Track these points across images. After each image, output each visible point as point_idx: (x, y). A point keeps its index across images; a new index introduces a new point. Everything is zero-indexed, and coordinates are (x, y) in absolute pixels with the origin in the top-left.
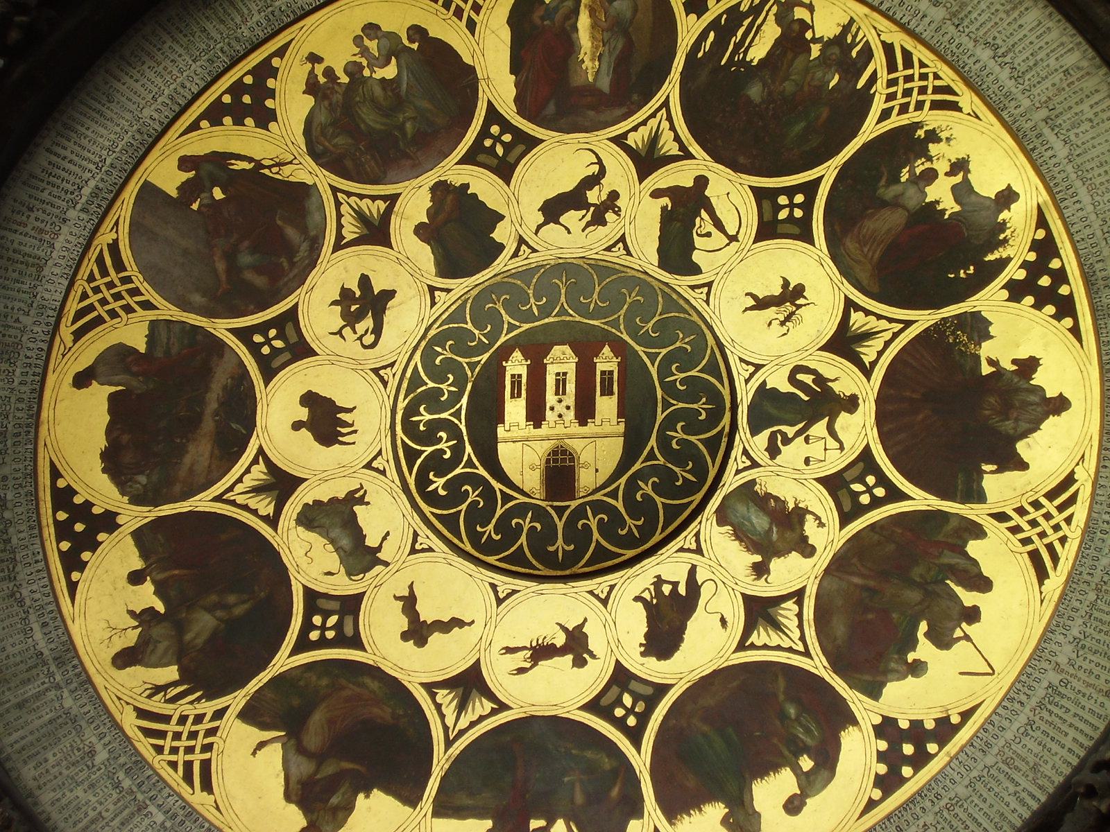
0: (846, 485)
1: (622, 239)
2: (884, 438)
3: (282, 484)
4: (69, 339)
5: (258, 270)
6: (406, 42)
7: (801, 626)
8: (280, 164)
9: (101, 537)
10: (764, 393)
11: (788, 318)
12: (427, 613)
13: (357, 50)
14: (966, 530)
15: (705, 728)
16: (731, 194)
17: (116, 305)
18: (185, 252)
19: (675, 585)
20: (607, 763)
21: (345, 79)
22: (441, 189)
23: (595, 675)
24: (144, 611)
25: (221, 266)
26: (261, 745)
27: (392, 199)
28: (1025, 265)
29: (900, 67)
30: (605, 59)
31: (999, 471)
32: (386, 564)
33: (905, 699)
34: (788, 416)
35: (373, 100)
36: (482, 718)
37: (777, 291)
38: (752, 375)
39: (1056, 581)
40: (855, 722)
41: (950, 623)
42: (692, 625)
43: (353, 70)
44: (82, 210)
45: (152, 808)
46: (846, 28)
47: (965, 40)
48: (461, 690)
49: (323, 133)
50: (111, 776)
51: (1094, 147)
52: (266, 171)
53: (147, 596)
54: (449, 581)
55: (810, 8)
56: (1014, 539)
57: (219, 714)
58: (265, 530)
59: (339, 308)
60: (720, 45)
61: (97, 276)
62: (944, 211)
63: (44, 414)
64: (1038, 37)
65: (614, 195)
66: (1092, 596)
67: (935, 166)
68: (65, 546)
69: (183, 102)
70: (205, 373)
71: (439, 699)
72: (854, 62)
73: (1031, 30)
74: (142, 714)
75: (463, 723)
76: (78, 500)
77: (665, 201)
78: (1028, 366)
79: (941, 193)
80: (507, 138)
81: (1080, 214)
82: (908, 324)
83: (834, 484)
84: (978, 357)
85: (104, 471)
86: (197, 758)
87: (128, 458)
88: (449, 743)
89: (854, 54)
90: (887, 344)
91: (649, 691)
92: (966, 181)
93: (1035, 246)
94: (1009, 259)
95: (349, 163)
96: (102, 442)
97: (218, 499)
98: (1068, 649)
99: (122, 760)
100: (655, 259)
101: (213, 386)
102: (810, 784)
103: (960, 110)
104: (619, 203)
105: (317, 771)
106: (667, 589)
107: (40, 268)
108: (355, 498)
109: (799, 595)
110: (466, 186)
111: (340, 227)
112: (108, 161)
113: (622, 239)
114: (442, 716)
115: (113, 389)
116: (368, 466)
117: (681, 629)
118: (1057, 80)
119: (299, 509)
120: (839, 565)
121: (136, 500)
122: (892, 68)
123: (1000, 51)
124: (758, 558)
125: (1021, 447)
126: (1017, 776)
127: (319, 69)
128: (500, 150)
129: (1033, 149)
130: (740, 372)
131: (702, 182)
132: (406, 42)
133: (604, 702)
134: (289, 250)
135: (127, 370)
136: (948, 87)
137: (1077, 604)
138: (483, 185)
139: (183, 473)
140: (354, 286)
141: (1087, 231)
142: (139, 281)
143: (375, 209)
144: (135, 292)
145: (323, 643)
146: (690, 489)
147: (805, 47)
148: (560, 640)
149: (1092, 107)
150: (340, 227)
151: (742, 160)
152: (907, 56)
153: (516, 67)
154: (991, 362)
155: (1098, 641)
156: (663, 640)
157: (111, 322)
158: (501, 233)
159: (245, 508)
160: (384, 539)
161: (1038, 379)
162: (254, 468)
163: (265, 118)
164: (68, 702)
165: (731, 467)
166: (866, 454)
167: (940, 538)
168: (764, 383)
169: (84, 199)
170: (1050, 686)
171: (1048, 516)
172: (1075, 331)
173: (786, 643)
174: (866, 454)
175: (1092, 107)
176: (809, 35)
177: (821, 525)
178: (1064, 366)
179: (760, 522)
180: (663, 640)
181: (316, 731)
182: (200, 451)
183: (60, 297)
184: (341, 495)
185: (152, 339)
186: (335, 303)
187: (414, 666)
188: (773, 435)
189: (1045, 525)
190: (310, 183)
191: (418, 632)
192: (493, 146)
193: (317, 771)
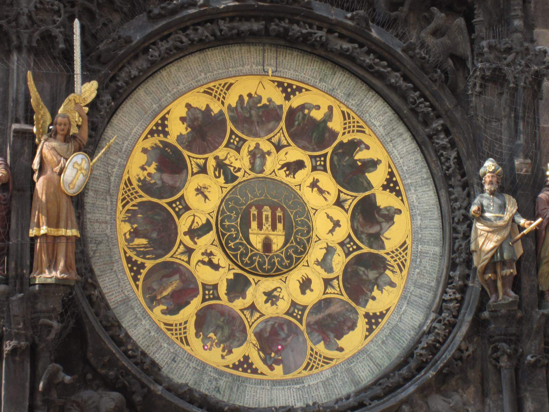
0: (236, 146)
1: (212, 244)
2: (220, 144)
3: (327, 283)
4: (334, 361)
5: (283, 330)
6: (202, 336)
7: (276, 134)
9: (371, 314)
10: (226, 182)
11: (205, 188)
12: (331, 225)
13: (213, 348)
14: (230, 109)
15: (313, 141)
16: (183, 224)
18: (292, 351)
19: (285, 171)
20: (335, 158)
21: (222, 345)
22: (231, 300)
24: (379, 290)
25: (289, 340)
26: (387, 239)
27: (242, 310)
28: (159, 136)
29: (126, 200)
30: (171, 281)
31: (212, 110)
32: (327, 244)
33: (278, 98)
34: (229, 172)
35: (222, 334)
36: (345, 194)
37: (200, 195)
38: (224, 188)
39: (231, 81)
40: (290, 106)
41: (254, 99)
43: (218, 345)
44: (303, 383)
45: (419, 250)
46: (125, 221)
49: (239, 341)
50: (420, 265)
53: (376, 292)
54: (320, 225)
55: (125, 234)
56: (226, 97)
57: (388, 254)
58: (341, 278)
59: (278, 303)
60: (148, 253)
61: (315, 367)
62: (156, 165)
63: (356, 351)
65: (203, 254)
66: (230, 69)
67: (146, 175)
68: (380, 320)
70: (316, 323)
71: (348, 207)
72: (132, 214)
74: (401, 270)
75: (349, 197)
76: (368, 326)
77: (196, 240)
78: (183, 119)
79: (152, 169)
82: (189, 157)
83: (238, 149)
84: (188, 134)
85: (356, 326)
86: (401, 250)
87: (349, 324)
88: (356, 197)
89: (130, 215)
90: (197, 158)
91: (313, 160)
92: (146, 164)
95: (241, 328)
96: (351, 332)
97: (342, 295)
98: (246, 67)
99: (414, 265)
100: (211, 232)
101: (317, 318)
102: (312, 107)
103: (129, 177)
104: (203, 251)
105: (383, 222)
106: (287, 172)
107: (325, 382)
108: (318, 263)
109: (269, 140)
110: (226, 294)
111: (258, 318)
112: (287, 387)
113: (212, 244)
114: (351, 203)
115: (337, 341)
116: (308, 266)
117: (294, 162)
119: (330, 274)
120: (256, 135)
121: (357, 313)
122: (128, 202)
124: (267, 156)
125: (203, 109)
126: (281, 61)
127: (224, 354)
128: (211, 292)
130: (225, 191)
131: (185, 234)
132: (202, 336)
133: (322, 168)
134: (273, 326)
135: (330, 341)
138: (222, 290)
139: (343, 308)
140: (269, 304)
141: (143, 124)
142: (308, 356)
143: (247, 313)
144: (311, 355)
145: (355, 244)
146: (223, 221)
147: (135, 229)
148: (315, 189)
150: (258, 318)
151: (173, 227)
152: (123, 200)
153: (188, 303)
156: (300, 165)
157: (323, 355)
158: (231, 276)
159: (339, 287)
160: (322, 249)
161: (184, 115)
162: (329, 292)
163: (246, 358)
164: (412, 288)
165: (249, 177)
166: (227, 146)
167: (236, 115)
168: (225, 183)
169: (301, 385)
170: (256, 66)
171: (216, 92)
173: (282, 135)
174: (227, 146)
176: (132, 230)
177: (249, 146)
178: (178, 110)
179: (258, 162)
180: (300, 165)
181: (374, 229)
182: (334, 309)
184: (319, 267)
185: (319, 342)
186: (277, 305)
187: (344, 218)
188: (236, 172)
189: (219, 91)
190: (252, 335)
191: (337, 224)
192: (211, 294)
193: (383, 222)
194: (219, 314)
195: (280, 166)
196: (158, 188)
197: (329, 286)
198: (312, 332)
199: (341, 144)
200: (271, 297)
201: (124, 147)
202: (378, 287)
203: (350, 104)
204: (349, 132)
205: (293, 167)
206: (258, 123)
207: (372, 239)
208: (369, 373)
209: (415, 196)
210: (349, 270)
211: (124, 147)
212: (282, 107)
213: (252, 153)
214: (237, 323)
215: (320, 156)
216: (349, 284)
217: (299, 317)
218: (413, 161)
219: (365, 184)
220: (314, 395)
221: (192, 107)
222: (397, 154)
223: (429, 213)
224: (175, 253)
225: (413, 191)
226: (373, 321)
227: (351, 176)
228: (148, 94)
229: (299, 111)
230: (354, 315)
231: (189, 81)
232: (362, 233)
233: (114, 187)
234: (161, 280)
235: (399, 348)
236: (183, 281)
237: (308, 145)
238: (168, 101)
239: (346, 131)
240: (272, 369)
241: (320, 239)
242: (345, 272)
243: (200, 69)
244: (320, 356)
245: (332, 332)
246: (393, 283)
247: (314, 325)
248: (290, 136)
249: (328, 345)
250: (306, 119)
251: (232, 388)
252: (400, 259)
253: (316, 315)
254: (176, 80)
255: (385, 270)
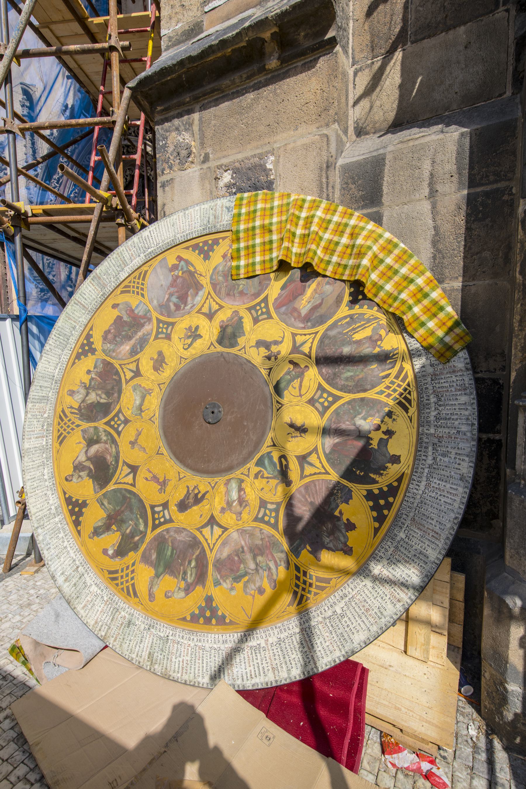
3: (137, 373)
5: (175, 305)
8: (201, 275)
9: (89, 354)
15: (170, 544)
17: (135, 290)
18: (162, 285)
19: (199, 492)
22: (236, 312)
23: (161, 499)
25: (167, 296)
26: (80, 443)
27: (221, 307)
28: (380, 489)
29: (400, 379)
31: (310, 552)
36: (128, 484)
37: (299, 425)
42: (195, 508)
44: (145, 256)
45: (45, 439)
47: (431, 388)
48: (130, 470)
50: (44, 422)
51: (443, 470)
52: (196, 275)
53: (86, 379)
56: (295, 581)
57: (78, 426)
64: (459, 409)
69: (189, 238)
70: (143, 325)
73: (459, 404)
74: (63, 411)
76: (91, 340)
78: (351, 526)
80: (264, 310)
81: (415, 491)
82: (327, 473)
84: (338, 506)
87: (110, 336)
88: (116, 483)
92: (387, 440)
93: (390, 486)
94: (377, 482)
95: (218, 287)
96: (107, 328)
97: (120, 365)
103: (407, 412)
106: (196, 491)
107: (125, 266)
108: (149, 392)
115: (119, 314)
116: (159, 385)
117: (190, 507)
118: (452, 432)
120: (242, 532)
121: (104, 351)
122: (397, 377)
123: (440, 403)
124: (225, 506)
128: (260, 312)
129: (420, 451)
134: (186, 305)
135: (126, 311)
136: (411, 400)
137: (291, 627)
139: (118, 351)
141: (412, 500)
148: (161, 480)
149: (456, 454)
154: (340, 512)
155: (286, 648)
156: (183, 506)
158: (241, 341)
159: (124, 373)
161: (350, 534)
163: (207, 257)
164: (50, 395)
167: (275, 555)
168: (271, 452)
172: (376, 530)
173: (209, 542)
175: (456, 454)
176: (379, 343)
179: (234, 495)
180: (183, 506)
182: (126, 348)
183: (123, 278)
185: (137, 307)
188: (260, 472)
194: (245, 292)
195: (207, 496)
196: (359, 414)
197: (135, 369)
198: (146, 315)
199: (136, 548)
200: (194, 334)
201: (430, 453)
202: (85, 386)
203: (127, 610)
204: (128, 568)
205: (191, 500)
206: (243, 552)
207: (95, 438)
208: (84, 292)
209: (51, 502)
210: (116, 395)
211: (430, 453)
212: (214, 583)
213: (244, 504)
214: (223, 290)
215: (161, 524)
216: (115, 380)
217: (161, 325)
218: (52, 547)
219: (106, 503)
220: (134, 249)
221: (342, 550)
222: (71, 552)
223: (36, 485)
224: (314, 339)
225: (53, 507)
226: (87, 348)
227: (122, 509)
228: (420, 553)
229: (192, 584)
230: (106, 348)
231: (358, 592)
232: (106, 442)
233: (426, 388)
234: (323, 300)
235: (59, 327)
236: (295, 310)
237: (176, 535)
238: (383, 550)
239: (131, 569)
240: (180, 258)
241: (150, 419)
242: (120, 392)
243: (346, 619)
244: (133, 292)
245: (125, 322)
246: (70, 395)
247: (145, 323)
248: (200, 543)
249: (127, 304)
250: (181, 573)
251: (215, 218)
252: (65, 424)
253: (144, 334)
254: (379, 590)
255: (80, 406)
